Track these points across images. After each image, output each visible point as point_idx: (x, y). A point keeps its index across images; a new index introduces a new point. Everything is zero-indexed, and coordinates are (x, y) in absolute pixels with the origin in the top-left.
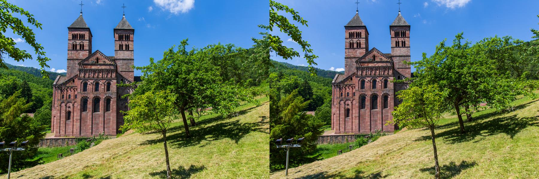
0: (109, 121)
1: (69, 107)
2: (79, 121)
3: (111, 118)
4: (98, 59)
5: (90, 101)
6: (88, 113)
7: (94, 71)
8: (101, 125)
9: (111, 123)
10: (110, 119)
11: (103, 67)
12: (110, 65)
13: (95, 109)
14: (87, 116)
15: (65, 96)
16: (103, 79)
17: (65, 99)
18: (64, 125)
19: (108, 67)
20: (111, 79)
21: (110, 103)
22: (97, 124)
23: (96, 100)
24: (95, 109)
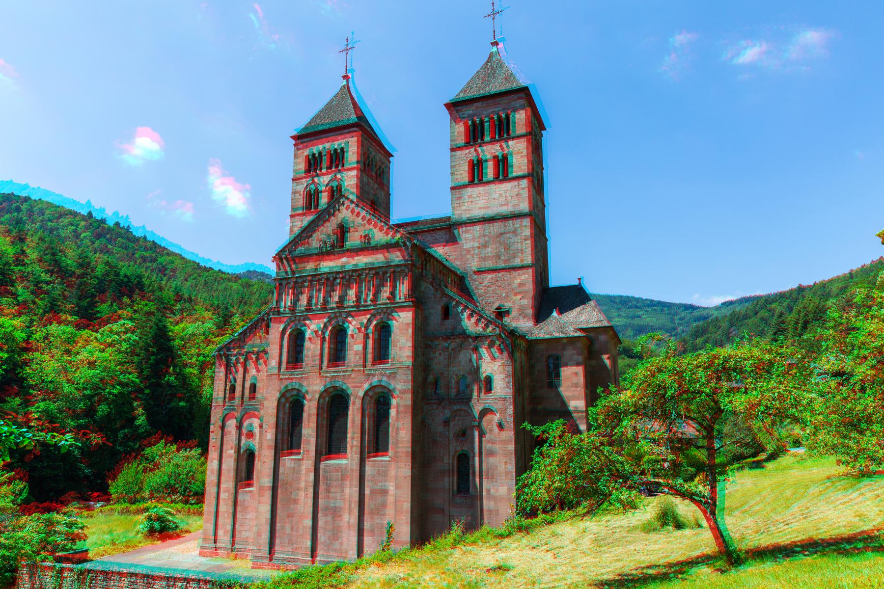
0: (380, 499)
1: (250, 435)
2: (268, 495)
3: (391, 487)
4: (343, 230)
5: (310, 409)
6: (300, 466)
7: (329, 281)
8: (349, 518)
9: (390, 511)
10: (384, 492)
11: (362, 261)
12: (388, 247)
13: (331, 444)
14: (296, 471)
15: (238, 389)
16: (359, 308)
17: (237, 402)
18: (231, 510)
19: (378, 259)
20: (393, 307)
21: (386, 415)
22: (335, 513)
23: (335, 403)
24: (331, 444)
